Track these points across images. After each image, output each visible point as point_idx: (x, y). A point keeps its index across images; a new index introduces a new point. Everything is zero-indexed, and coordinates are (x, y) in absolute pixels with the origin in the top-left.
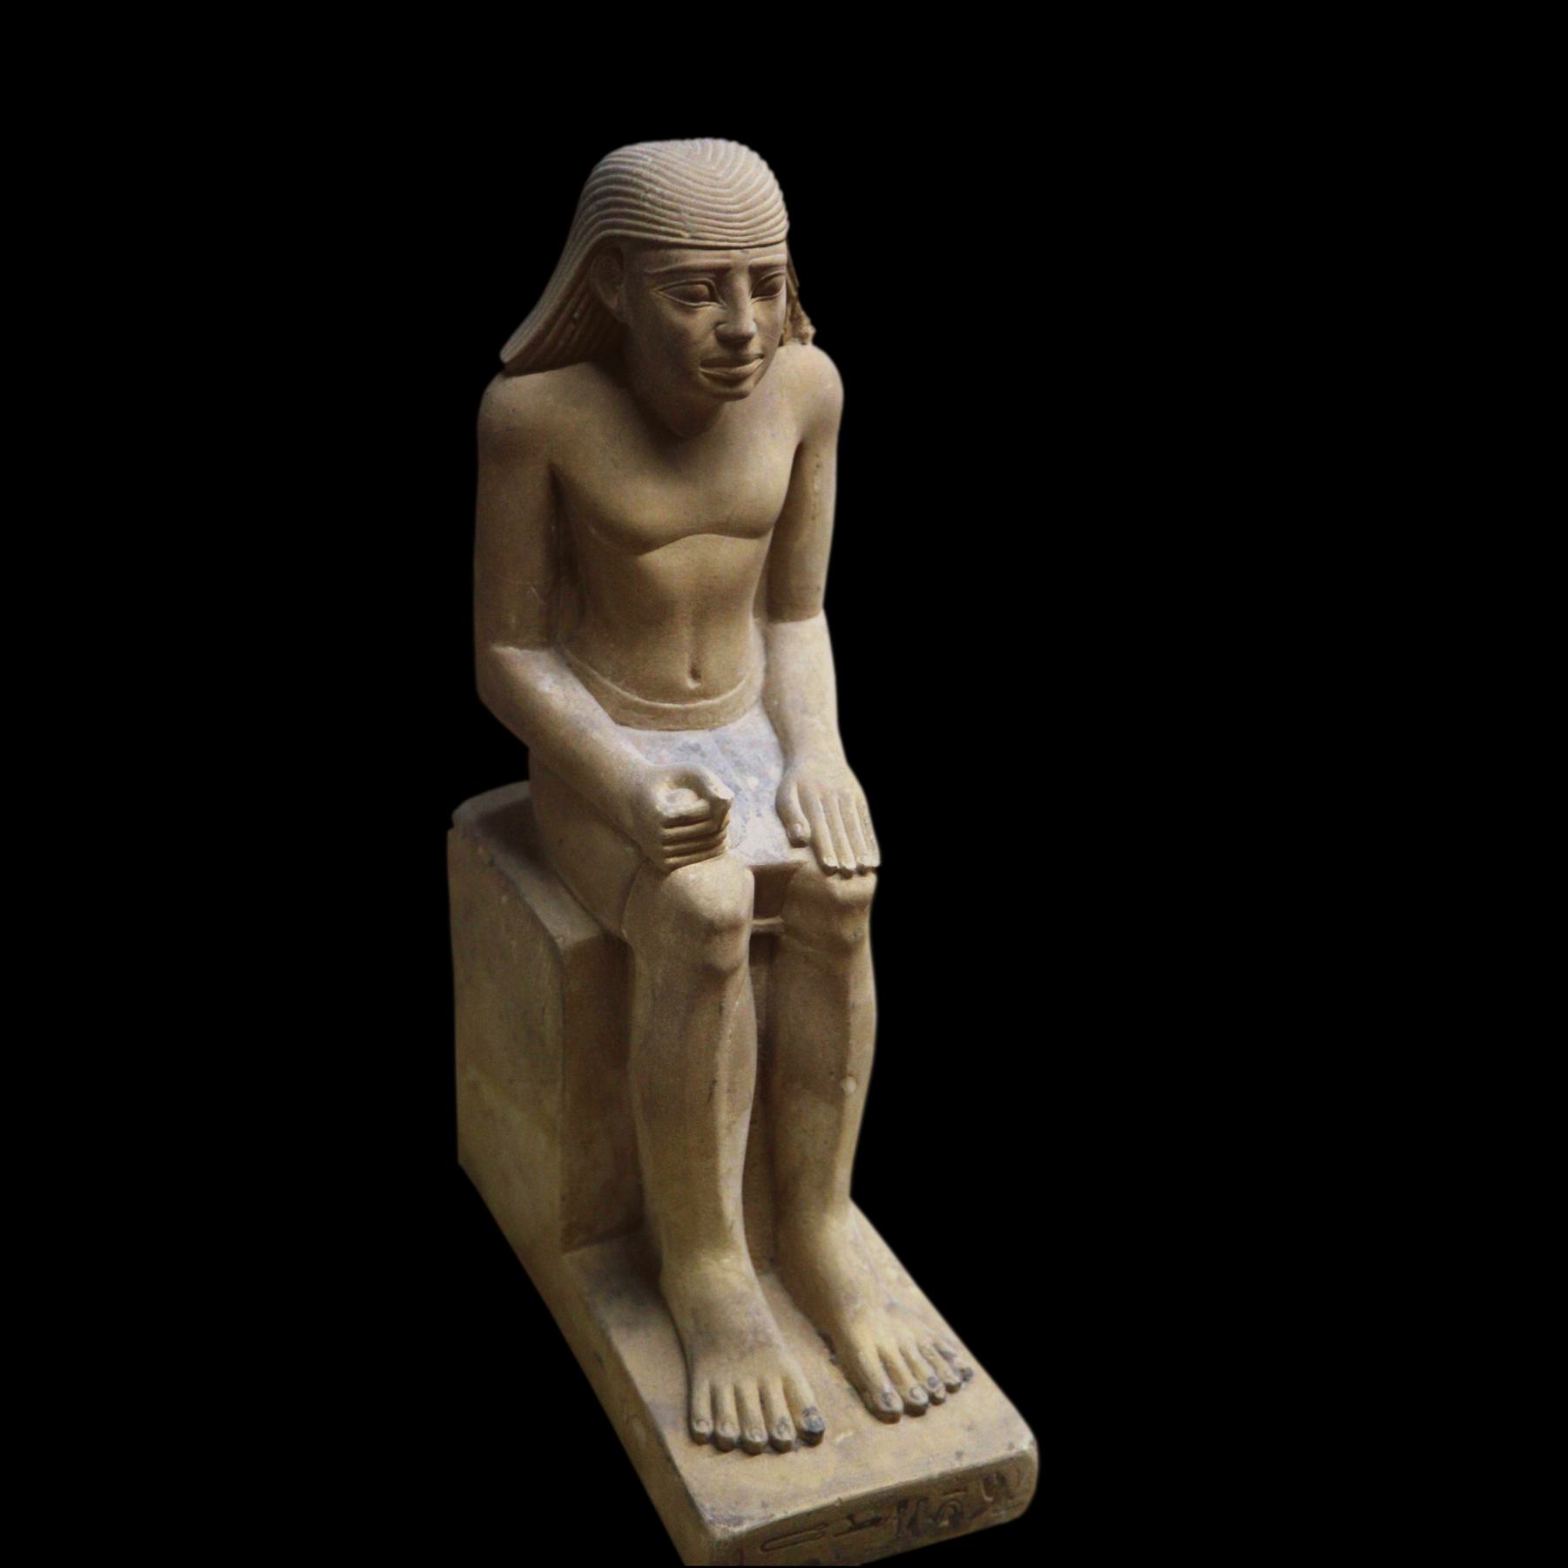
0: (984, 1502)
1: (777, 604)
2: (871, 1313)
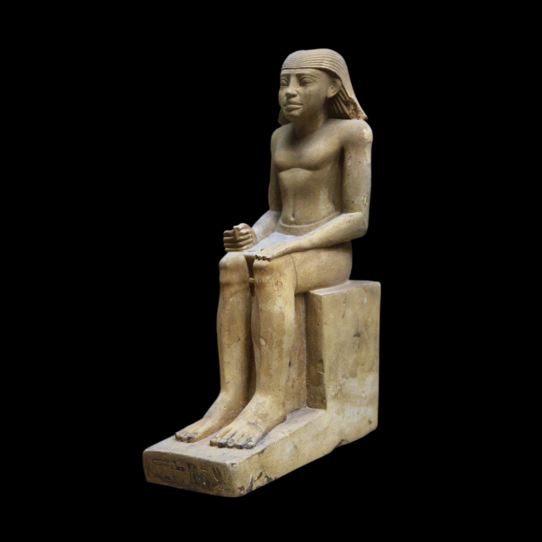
0: (214, 480)
1: (342, 205)
2: (241, 420)
